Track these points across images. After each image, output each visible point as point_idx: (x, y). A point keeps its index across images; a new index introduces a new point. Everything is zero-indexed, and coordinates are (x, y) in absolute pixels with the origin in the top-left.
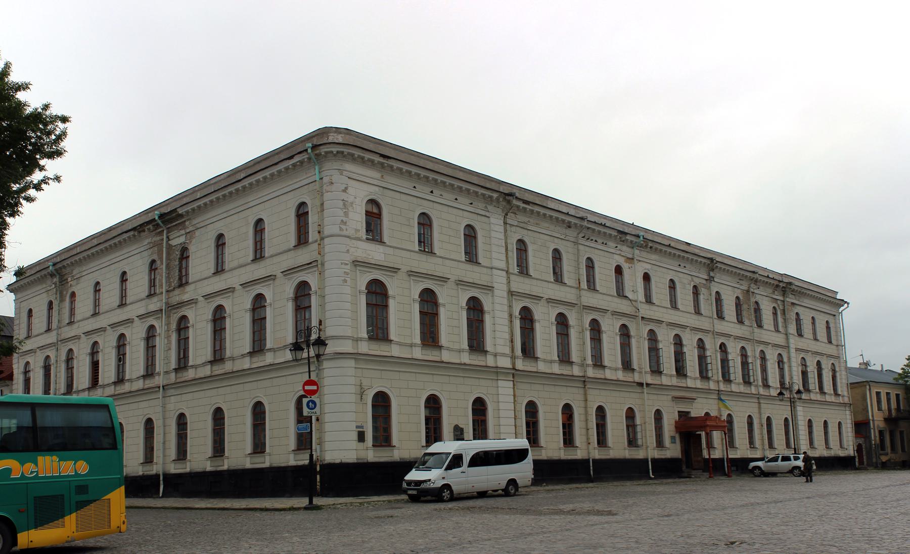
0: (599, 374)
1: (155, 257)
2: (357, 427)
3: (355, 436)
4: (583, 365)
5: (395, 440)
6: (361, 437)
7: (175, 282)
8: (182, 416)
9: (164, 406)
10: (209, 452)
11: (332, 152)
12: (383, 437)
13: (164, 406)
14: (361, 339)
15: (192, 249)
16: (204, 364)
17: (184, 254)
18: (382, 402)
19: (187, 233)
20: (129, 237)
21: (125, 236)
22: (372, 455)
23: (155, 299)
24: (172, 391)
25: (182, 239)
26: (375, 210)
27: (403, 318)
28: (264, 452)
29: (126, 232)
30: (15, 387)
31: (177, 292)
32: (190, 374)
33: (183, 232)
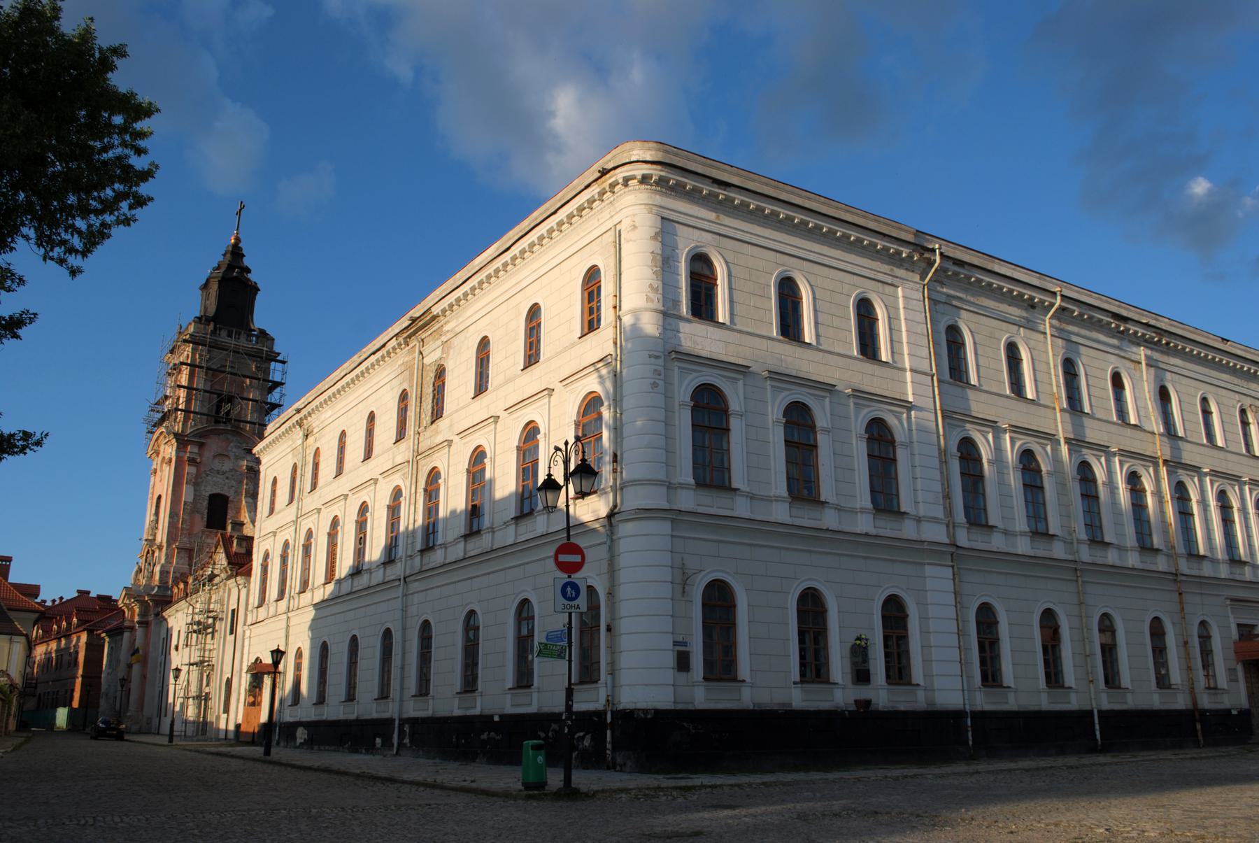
0: (1099, 557)
1: (405, 386)
2: (676, 643)
3: (670, 659)
4: (1068, 543)
5: (744, 668)
6: (683, 662)
7: (427, 418)
8: (426, 625)
9: (404, 610)
10: (458, 684)
11: (633, 178)
12: (721, 665)
13: (404, 610)
14: (683, 486)
15: (449, 366)
16: (456, 541)
17: (440, 373)
18: (719, 602)
19: (444, 343)
20: (378, 361)
21: (373, 358)
22: (701, 696)
23: (403, 445)
24: (416, 584)
25: (438, 354)
26: (707, 272)
27: (757, 450)
28: (529, 686)
29: (374, 353)
30: (252, 585)
31: (428, 433)
32: (438, 557)
33: (439, 342)
